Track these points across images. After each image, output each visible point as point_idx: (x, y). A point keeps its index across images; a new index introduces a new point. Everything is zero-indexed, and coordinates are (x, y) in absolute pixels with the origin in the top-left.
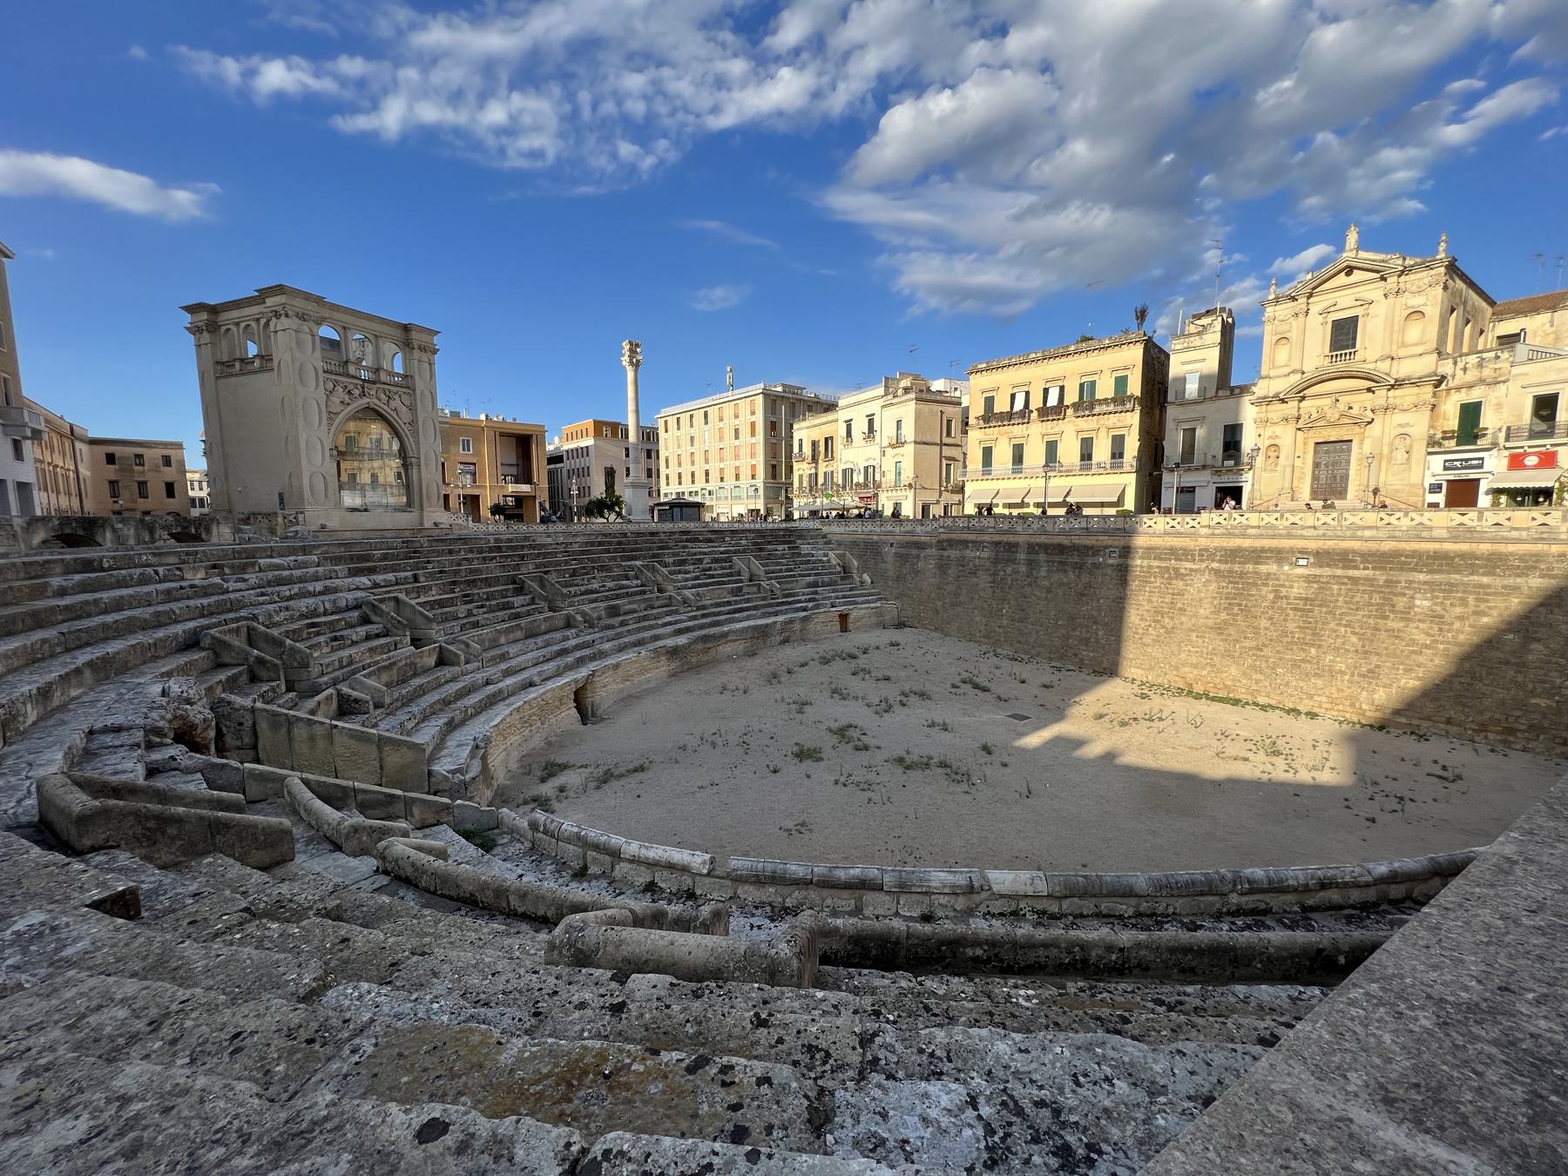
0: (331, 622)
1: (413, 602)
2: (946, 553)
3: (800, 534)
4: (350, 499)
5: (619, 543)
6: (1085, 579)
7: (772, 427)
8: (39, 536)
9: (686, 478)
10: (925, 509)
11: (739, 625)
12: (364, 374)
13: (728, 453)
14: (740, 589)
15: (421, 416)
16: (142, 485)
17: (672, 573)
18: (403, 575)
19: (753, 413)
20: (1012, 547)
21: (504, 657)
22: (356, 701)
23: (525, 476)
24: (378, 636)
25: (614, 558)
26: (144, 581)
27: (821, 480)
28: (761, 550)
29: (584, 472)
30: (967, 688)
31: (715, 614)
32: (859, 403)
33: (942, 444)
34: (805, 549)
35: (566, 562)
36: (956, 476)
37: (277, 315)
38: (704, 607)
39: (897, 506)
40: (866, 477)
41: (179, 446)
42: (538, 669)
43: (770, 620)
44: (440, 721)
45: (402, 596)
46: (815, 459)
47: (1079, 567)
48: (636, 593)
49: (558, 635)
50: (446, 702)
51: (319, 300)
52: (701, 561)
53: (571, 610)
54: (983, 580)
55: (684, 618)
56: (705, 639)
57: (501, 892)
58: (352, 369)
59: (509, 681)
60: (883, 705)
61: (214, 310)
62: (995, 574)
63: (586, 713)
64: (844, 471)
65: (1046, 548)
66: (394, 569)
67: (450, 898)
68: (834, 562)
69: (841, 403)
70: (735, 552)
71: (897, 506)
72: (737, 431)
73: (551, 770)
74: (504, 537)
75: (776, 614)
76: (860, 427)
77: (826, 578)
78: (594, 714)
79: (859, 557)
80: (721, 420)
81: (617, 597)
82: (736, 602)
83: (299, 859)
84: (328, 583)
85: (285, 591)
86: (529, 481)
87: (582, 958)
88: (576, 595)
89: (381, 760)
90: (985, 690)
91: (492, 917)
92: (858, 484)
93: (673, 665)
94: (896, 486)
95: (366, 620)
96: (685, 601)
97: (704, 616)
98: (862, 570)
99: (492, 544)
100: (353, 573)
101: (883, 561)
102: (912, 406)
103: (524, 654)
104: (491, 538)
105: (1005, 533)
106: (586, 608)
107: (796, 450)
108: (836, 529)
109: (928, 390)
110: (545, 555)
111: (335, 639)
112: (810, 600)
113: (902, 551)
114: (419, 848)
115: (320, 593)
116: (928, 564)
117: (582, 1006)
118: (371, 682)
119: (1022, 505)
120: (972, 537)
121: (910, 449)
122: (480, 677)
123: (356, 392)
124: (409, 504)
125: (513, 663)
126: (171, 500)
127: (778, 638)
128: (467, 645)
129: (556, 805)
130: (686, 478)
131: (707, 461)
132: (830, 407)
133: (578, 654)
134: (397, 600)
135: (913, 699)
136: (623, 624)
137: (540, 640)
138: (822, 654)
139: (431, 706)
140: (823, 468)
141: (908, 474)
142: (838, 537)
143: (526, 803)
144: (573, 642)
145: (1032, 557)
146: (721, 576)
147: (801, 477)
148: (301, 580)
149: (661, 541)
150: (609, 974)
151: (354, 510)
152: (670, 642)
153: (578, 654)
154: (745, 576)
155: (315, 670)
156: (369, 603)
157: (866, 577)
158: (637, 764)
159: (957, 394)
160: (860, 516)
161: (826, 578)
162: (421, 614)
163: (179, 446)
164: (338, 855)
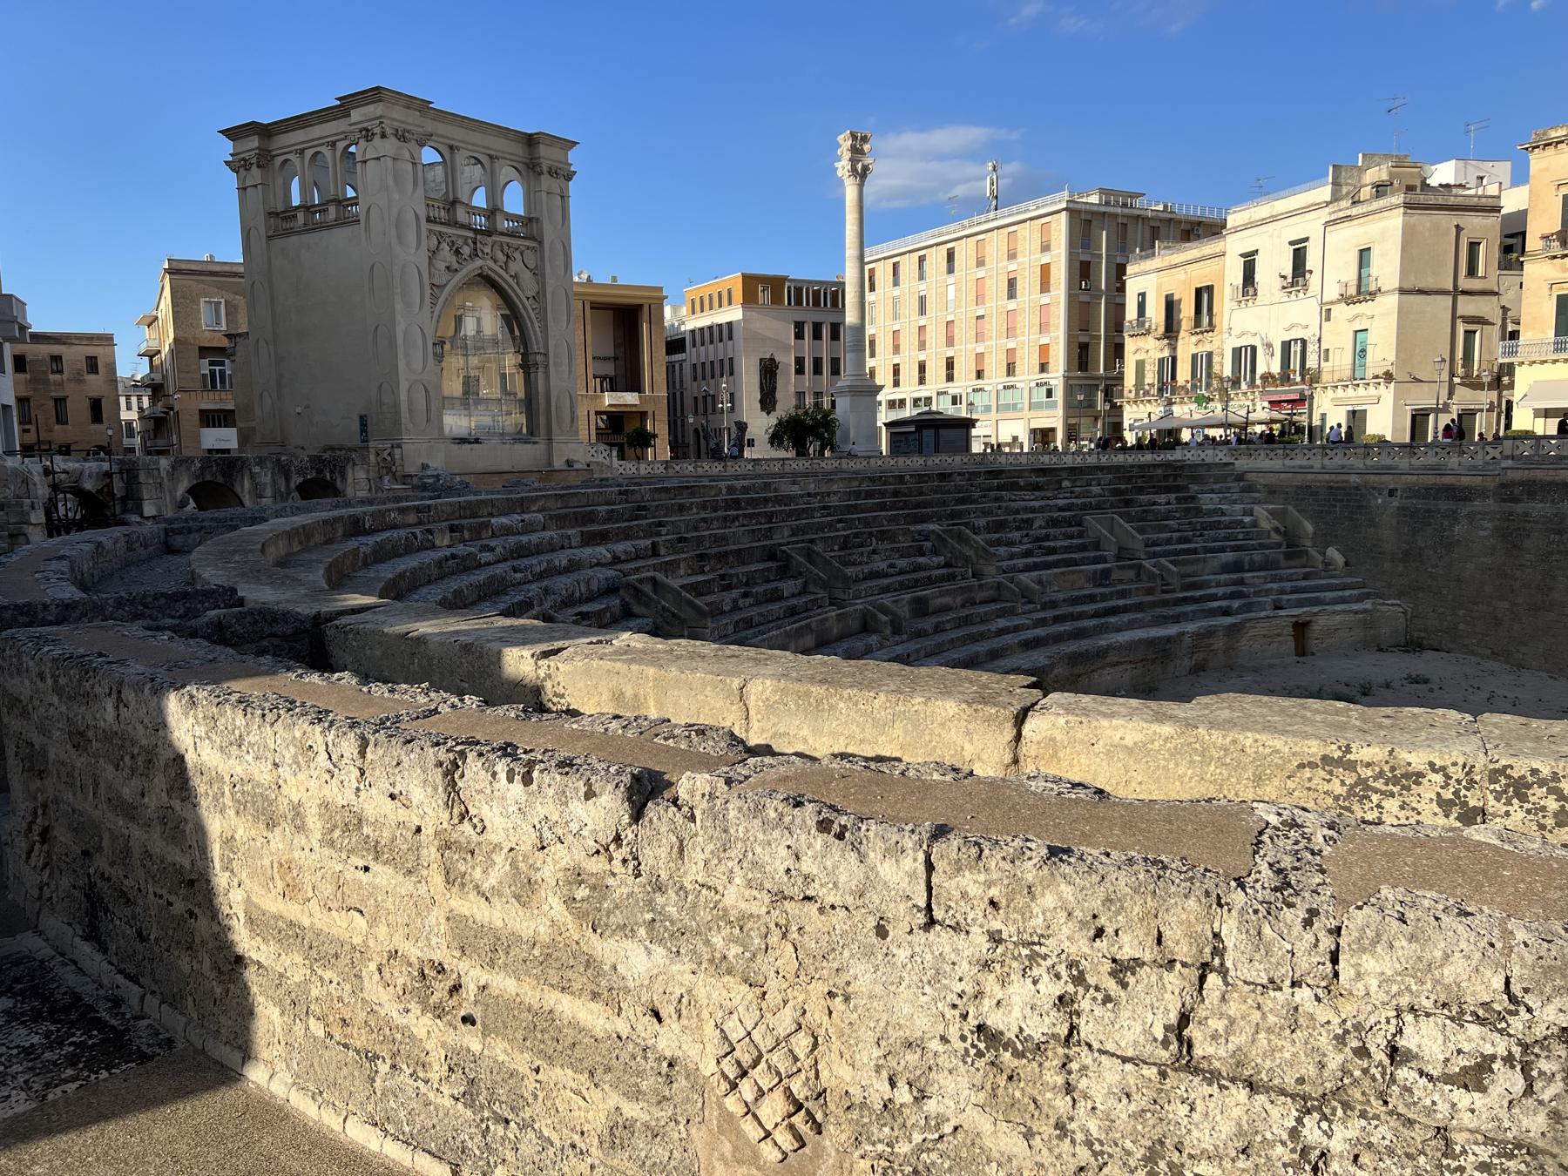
0: (600, 613)
1: (675, 583)
2: (1519, 508)
4: (456, 422)
5: (896, 493)
7: (1082, 271)
8: (183, 485)
9: (909, 374)
10: (1419, 419)
12: (480, 221)
13: (994, 326)
14: (1106, 574)
15: (551, 283)
16: (60, 402)
17: (991, 543)
19: (1046, 248)
25: (894, 519)
26: (409, 549)
27: (1183, 374)
28: (1128, 503)
29: (728, 367)
32: (1274, 219)
33: (1457, 292)
34: (1208, 501)
35: (831, 525)
36: (1488, 350)
37: (368, 135)
38: (1052, 604)
39: (1357, 417)
41: (107, 340)
43: (1172, 630)
48: (942, 579)
51: (423, 106)
52: (1029, 522)
58: (461, 215)
61: (265, 131)
64: (1237, 352)
66: (627, 535)
68: (1265, 525)
69: (1233, 220)
70: (1084, 507)
71: (1357, 417)
72: (1012, 283)
74: (739, 484)
75: (1176, 619)
76: (1273, 266)
77: (1257, 556)
80: (980, 263)
81: (916, 584)
82: (1104, 597)
85: (538, 563)
86: (636, 386)
92: (1267, 377)
94: (1355, 378)
96: (1026, 595)
97: (1057, 619)
98: (1323, 541)
100: (589, 539)
102: (1394, 221)
107: (1131, 313)
108: (1265, 463)
109: (1425, 186)
110: (798, 514)
113: (1420, 504)
115: (567, 570)
121: (1388, 304)
123: (466, 250)
124: (532, 430)
126: (97, 426)
130: (909, 374)
131: (950, 342)
132: (1215, 229)
134: (654, 581)
136: (939, 629)
140: (1187, 346)
141: (1383, 353)
142: (1272, 479)
146: (1067, 549)
147: (1140, 365)
148: (538, 550)
149: (959, 489)
151: (462, 441)
156: (628, 585)
157: (1333, 553)
159: (1492, 190)
160: (1268, 438)
162: (691, 604)
163: (107, 340)
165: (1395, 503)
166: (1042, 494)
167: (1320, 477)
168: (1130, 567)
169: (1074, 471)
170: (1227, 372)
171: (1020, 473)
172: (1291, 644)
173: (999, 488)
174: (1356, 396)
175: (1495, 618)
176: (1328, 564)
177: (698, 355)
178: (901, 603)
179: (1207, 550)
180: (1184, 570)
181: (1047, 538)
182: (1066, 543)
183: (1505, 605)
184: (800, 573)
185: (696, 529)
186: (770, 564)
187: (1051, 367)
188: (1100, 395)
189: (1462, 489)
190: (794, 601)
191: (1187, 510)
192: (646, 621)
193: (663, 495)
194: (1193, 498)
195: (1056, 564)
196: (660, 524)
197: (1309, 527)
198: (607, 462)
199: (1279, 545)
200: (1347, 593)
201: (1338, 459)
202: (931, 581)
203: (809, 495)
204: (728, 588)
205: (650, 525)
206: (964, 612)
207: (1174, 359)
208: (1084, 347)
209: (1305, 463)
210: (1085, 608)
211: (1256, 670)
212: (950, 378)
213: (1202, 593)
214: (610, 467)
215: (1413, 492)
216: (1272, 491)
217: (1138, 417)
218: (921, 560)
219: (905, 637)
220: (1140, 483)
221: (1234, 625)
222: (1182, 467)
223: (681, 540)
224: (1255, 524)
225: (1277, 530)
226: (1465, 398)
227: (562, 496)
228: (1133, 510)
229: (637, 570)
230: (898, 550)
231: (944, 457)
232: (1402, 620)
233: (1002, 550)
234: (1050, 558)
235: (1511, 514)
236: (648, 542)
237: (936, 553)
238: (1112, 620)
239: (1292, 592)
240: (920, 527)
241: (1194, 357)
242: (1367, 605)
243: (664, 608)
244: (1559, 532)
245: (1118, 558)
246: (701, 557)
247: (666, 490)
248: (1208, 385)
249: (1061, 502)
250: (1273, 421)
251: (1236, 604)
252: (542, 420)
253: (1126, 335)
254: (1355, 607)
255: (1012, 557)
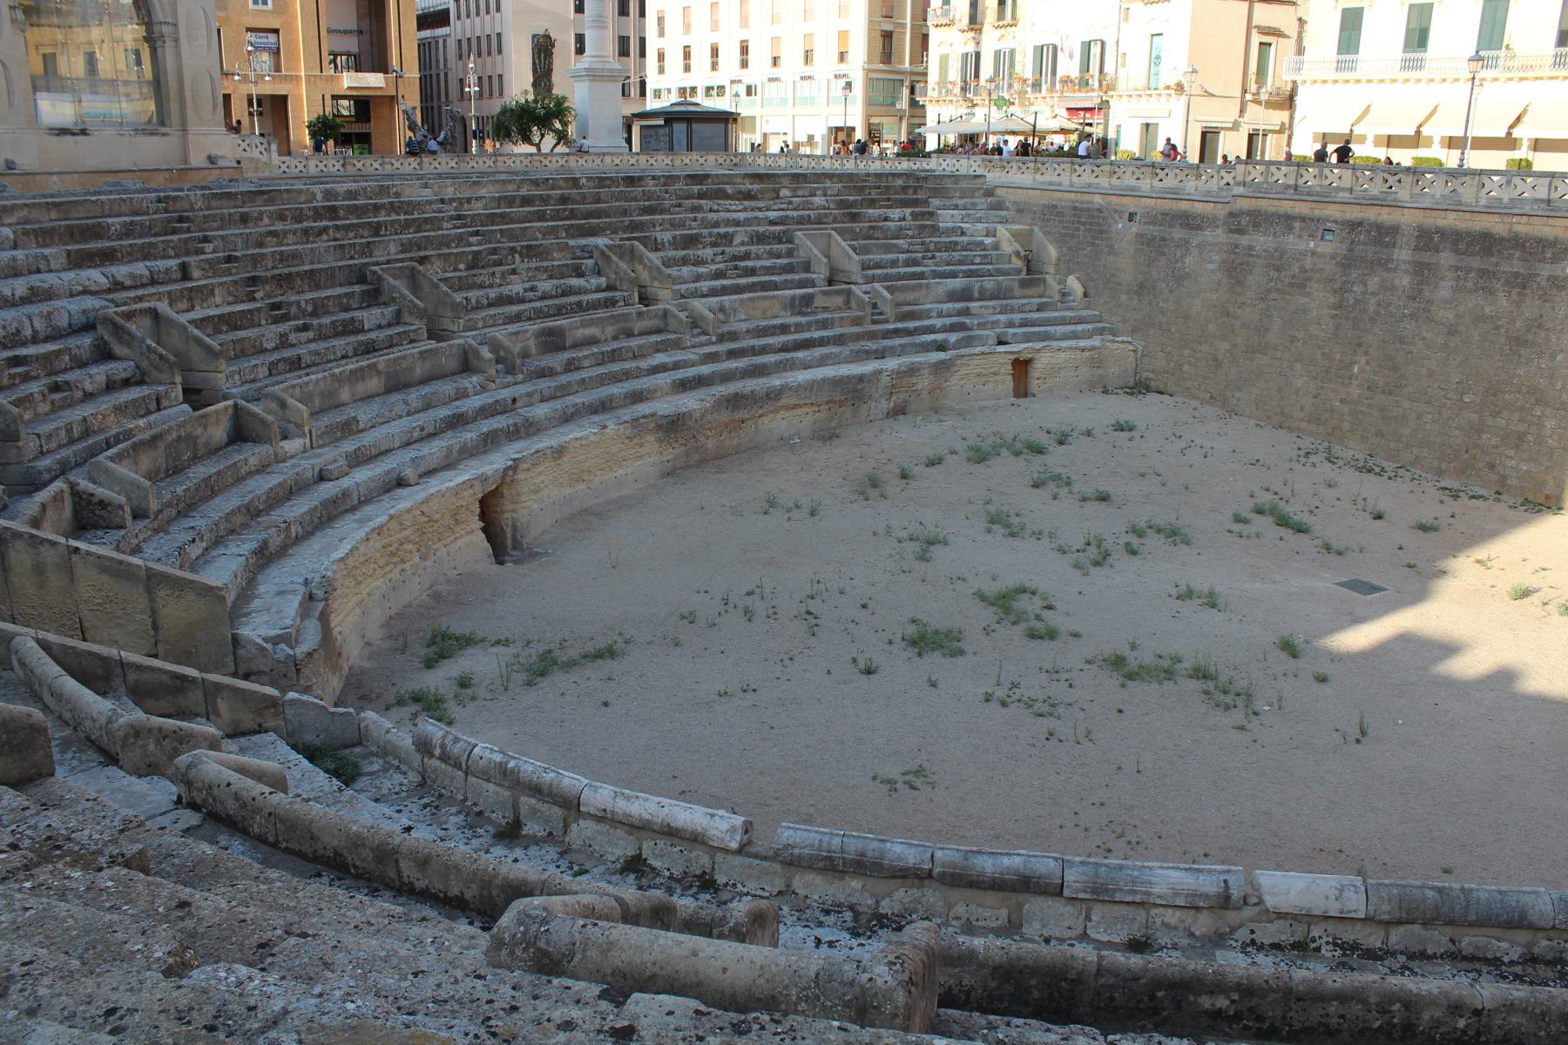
0: (47, 357)
1: (183, 319)
2: (1244, 240)
3: (939, 186)
5: (564, 200)
6: (1531, 308)
9: (701, 58)
10: (1208, 137)
11: (802, 376)
14: (808, 300)
17: (668, 263)
18: (162, 264)
20: (1384, 234)
21: (348, 429)
22: (103, 504)
23: (374, 56)
24: (127, 383)
25: (552, 231)
27: (987, 70)
28: (854, 218)
29: (492, 45)
30: (1265, 523)
31: (754, 351)
34: (948, 218)
35: (460, 240)
38: (733, 336)
40: (1085, 66)
42: (411, 453)
43: (868, 367)
44: (245, 546)
45: (163, 307)
46: (975, 20)
47: (1520, 283)
49: (446, 387)
50: (252, 512)
52: (728, 238)
53: (469, 339)
54: (1318, 300)
55: (691, 357)
56: (735, 401)
57: (386, 854)
59: (362, 475)
60: (1092, 552)
62: (1343, 290)
63: (501, 541)
64: (1040, 50)
65: (1454, 238)
66: (146, 254)
67: (301, 855)
68: (1008, 247)
70: (800, 221)
73: (443, 647)
74: (341, 188)
75: (881, 355)
77: (989, 283)
78: (516, 545)
79: (1061, 240)
81: (560, 311)
82: (799, 328)
83: (60, 772)
84: (35, 280)
86: (381, 66)
87: (549, 964)
88: (479, 307)
89: (154, 612)
90: (1301, 529)
91: (374, 892)
92: (1066, 81)
93: (669, 454)
95: (104, 354)
96: (695, 323)
97: (732, 354)
98: (1067, 265)
99: (320, 202)
100: (78, 261)
101: (1112, 251)
103: (386, 422)
104: (317, 189)
105: (1374, 203)
106: (500, 334)
108: (1018, 178)
110: (419, 225)
111: (56, 388)
112: (952, 328)
114: (242, 770)
115: (25, 301)
116: (1204, 260)
117: (568, 1026)
118: (123, 470)
119: (1415, 140)
120: (1302, 208)
122: (309, 465)
125: (367, 439)
127: (884, 406)
128: (283, 405)
129: (453, 710)
130: (701, 58)
133: (486, 426)
134: (154, 314)
135: (1153, 541)
136: (570, 367)
137: (414, 397)
138: (973, 441)
139: (228, 517)
140: (992, 39)
142: (1020, 196)
143: (401, 702)
144: (474, 403)
145: (1426, 257)
146: (769, 270)
147: (944, 60)
149: (649, 196)
150: (596, 989)
152: (664, 406)
153: (486, 426)
154: (820, 273)
155: (30, 445)
156: (107, 320)
157: (1074, 284)
158: (601, 643)
161: (989, 283)
162: (199, 342)
164: (112, 771)
165: (1134, 228)
166: (753, 204)
167: (1067, 196)
168: (838, 293)
169: (797, 178)
170: (1028, 73)
171: (730, 179)
172: (1010, 384)
173: (701, 196)
174: (1152, 109)
175: (1216, 360)
176: (1064, 294)
177: (464, 31)
178: (520, 336)
179: (935, 275)
180: (900, 297)
181: (747, 256)
182: (767, 263)
183: (1225, 346)
184: (394, 300)
185: (261, 245)
186: (357, 288)
187: (850, 57)
188: (906, 92)
189: (1195, 217)
190: (373, 335)
191: (923, 227)
192: (120, 365)
193: (225, 202)
194: (931, 214)
195: (751, 288)
196: (206, 240)
197: (1052, 252)
198: (265, 158)
199: (1019, 271)
200: (1080, 327)
201: (1085, 176)
202: (579, 307)
203: (442, 201)
204: (285, 318)
205: (186, 241)
206: (616, 345)
207: (978, 55)
208: (888, 36)
209: (1054, 179)
210: (770, 340)
211: (961, 414)
212: (744, 64)
213: (917, 324)
214: (268, 164)
215: (1155, 218)
216: (1021, 210)
217: (943, 117)
218: (575, 282)
219: (520, 377)
220: (874, 195)
221: (943, 362)
222: (926, 178)
223: (229, 259)
224: (996, 247)
225: (1017, 254)
226: (1260, 118)
227: (56, 205)
228: (857, 226)
229: (140, 299)
230: (546, 269)
231: (694, 156)
232: (1132, 359)
233: (686, 271)
234: (743, 281)
235: (1237, 246)
236: (173, 263)
237: (599, 274)
238: (800, 354)
239: (1022, 325)
240: (583, 241)
241: (997, 54)
242: (1096, 341)
243: (149, 348)
244: (1278, 269)
245: (830, 282)
246: (253, 280)
247: (230, 196)
248: (1010, 86)
249: (772, 215)
250: (1063, 131)
251: (953, 337)
252: (174, 107)
253: (929, 23)
254: (1083, 343)
255: (698, 278)
